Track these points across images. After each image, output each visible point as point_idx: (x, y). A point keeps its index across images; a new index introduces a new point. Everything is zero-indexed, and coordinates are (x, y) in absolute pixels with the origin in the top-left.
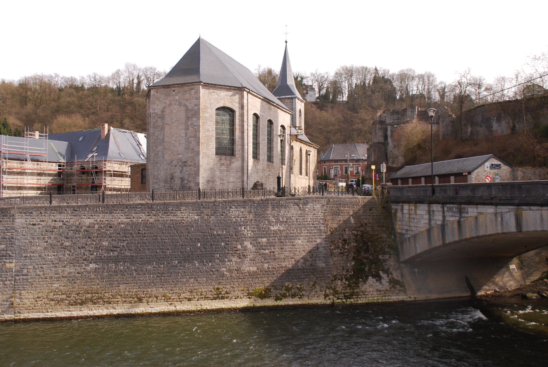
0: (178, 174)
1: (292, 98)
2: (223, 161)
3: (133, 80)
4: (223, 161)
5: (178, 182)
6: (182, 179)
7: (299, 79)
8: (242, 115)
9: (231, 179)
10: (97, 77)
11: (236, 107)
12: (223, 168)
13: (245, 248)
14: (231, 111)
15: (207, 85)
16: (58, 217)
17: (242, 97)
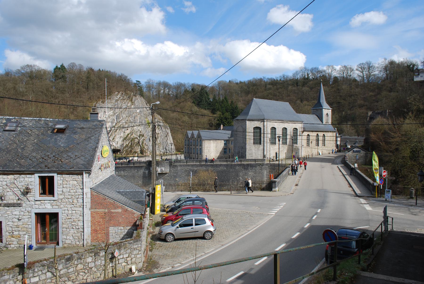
0: (241, 151)
1: (321, 109)
2: (256, 147)
3: (305, 76)
4: (256, 147)
5: (241, 154)
6: (242, 153)
7: (411, 66)
8: (264, 129)
9: (259, 153)
10: (285, 77)
11: (262, 127)
12: (256, 149)
13: (239, 179)
14: (260, 128)
15: (249, 120)
16: (188, 167)
17: (264, 123)
